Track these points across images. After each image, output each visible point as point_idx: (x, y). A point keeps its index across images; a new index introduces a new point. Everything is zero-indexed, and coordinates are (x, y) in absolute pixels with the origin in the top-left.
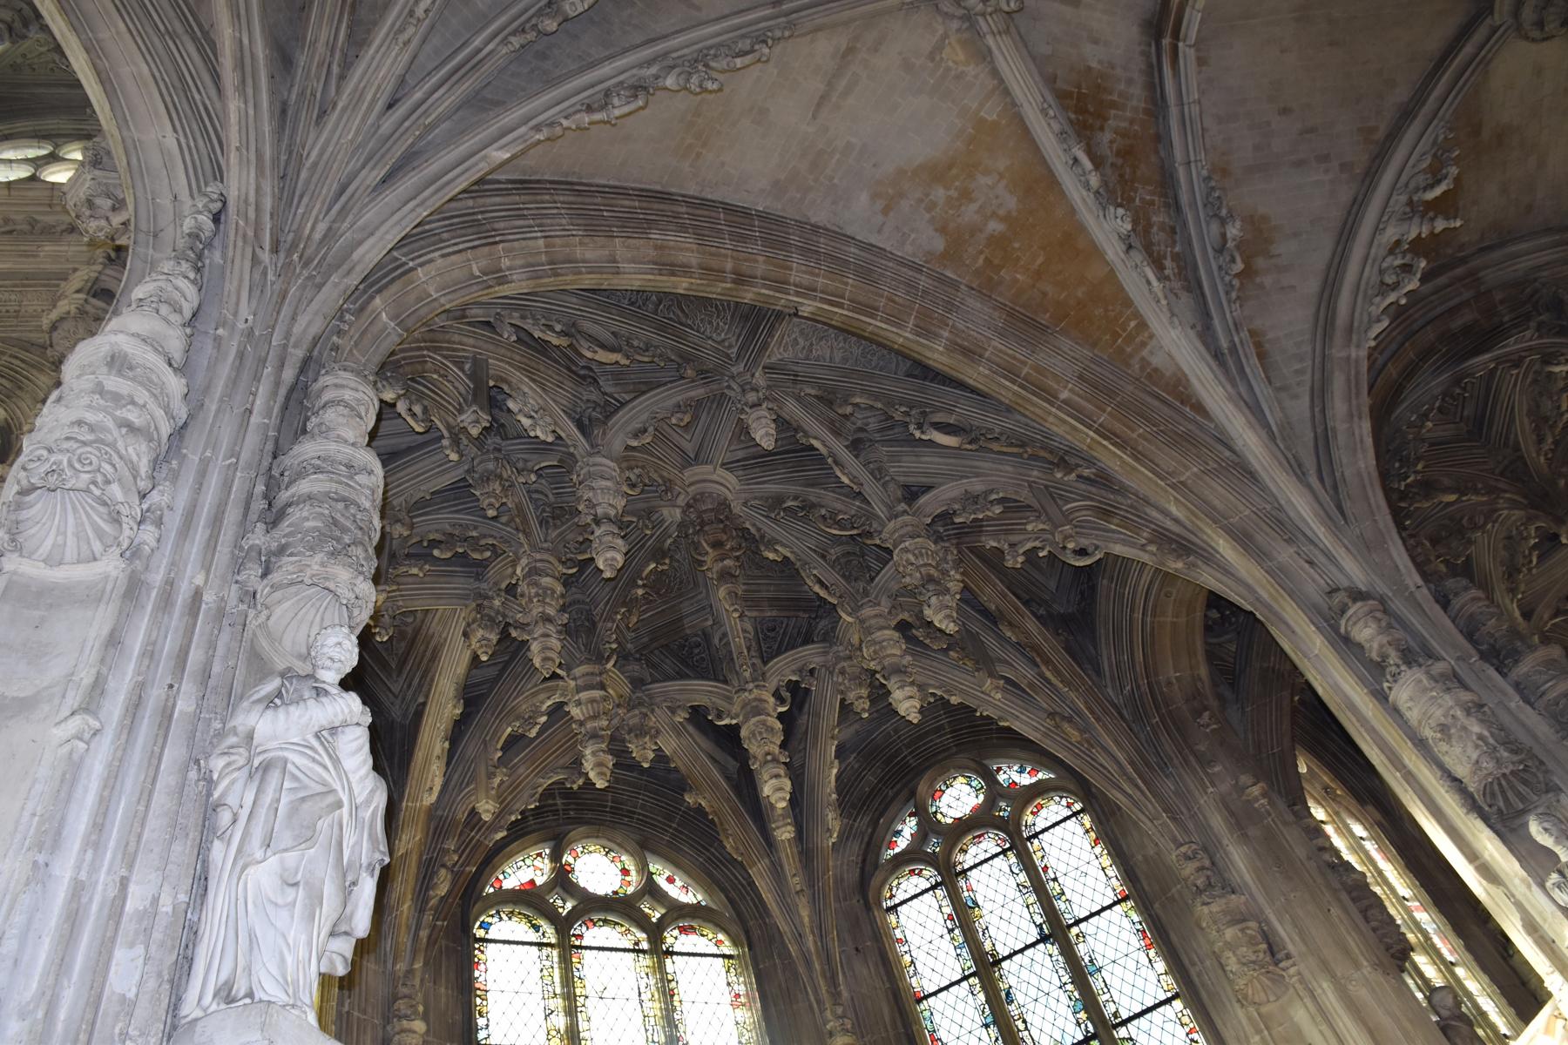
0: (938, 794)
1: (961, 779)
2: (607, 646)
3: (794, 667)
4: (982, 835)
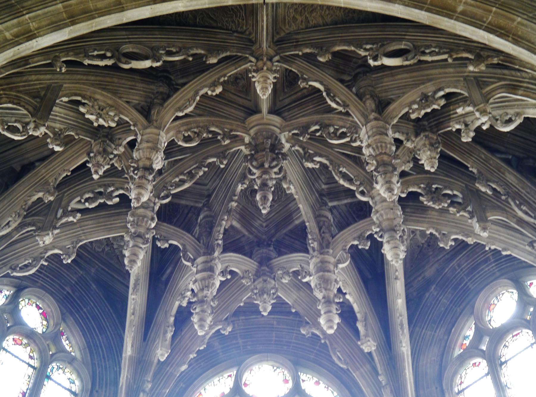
0: (492, 307)
1: (506, 294)
2: (216, 242)
3: (355, 235)
4: (519, 334)
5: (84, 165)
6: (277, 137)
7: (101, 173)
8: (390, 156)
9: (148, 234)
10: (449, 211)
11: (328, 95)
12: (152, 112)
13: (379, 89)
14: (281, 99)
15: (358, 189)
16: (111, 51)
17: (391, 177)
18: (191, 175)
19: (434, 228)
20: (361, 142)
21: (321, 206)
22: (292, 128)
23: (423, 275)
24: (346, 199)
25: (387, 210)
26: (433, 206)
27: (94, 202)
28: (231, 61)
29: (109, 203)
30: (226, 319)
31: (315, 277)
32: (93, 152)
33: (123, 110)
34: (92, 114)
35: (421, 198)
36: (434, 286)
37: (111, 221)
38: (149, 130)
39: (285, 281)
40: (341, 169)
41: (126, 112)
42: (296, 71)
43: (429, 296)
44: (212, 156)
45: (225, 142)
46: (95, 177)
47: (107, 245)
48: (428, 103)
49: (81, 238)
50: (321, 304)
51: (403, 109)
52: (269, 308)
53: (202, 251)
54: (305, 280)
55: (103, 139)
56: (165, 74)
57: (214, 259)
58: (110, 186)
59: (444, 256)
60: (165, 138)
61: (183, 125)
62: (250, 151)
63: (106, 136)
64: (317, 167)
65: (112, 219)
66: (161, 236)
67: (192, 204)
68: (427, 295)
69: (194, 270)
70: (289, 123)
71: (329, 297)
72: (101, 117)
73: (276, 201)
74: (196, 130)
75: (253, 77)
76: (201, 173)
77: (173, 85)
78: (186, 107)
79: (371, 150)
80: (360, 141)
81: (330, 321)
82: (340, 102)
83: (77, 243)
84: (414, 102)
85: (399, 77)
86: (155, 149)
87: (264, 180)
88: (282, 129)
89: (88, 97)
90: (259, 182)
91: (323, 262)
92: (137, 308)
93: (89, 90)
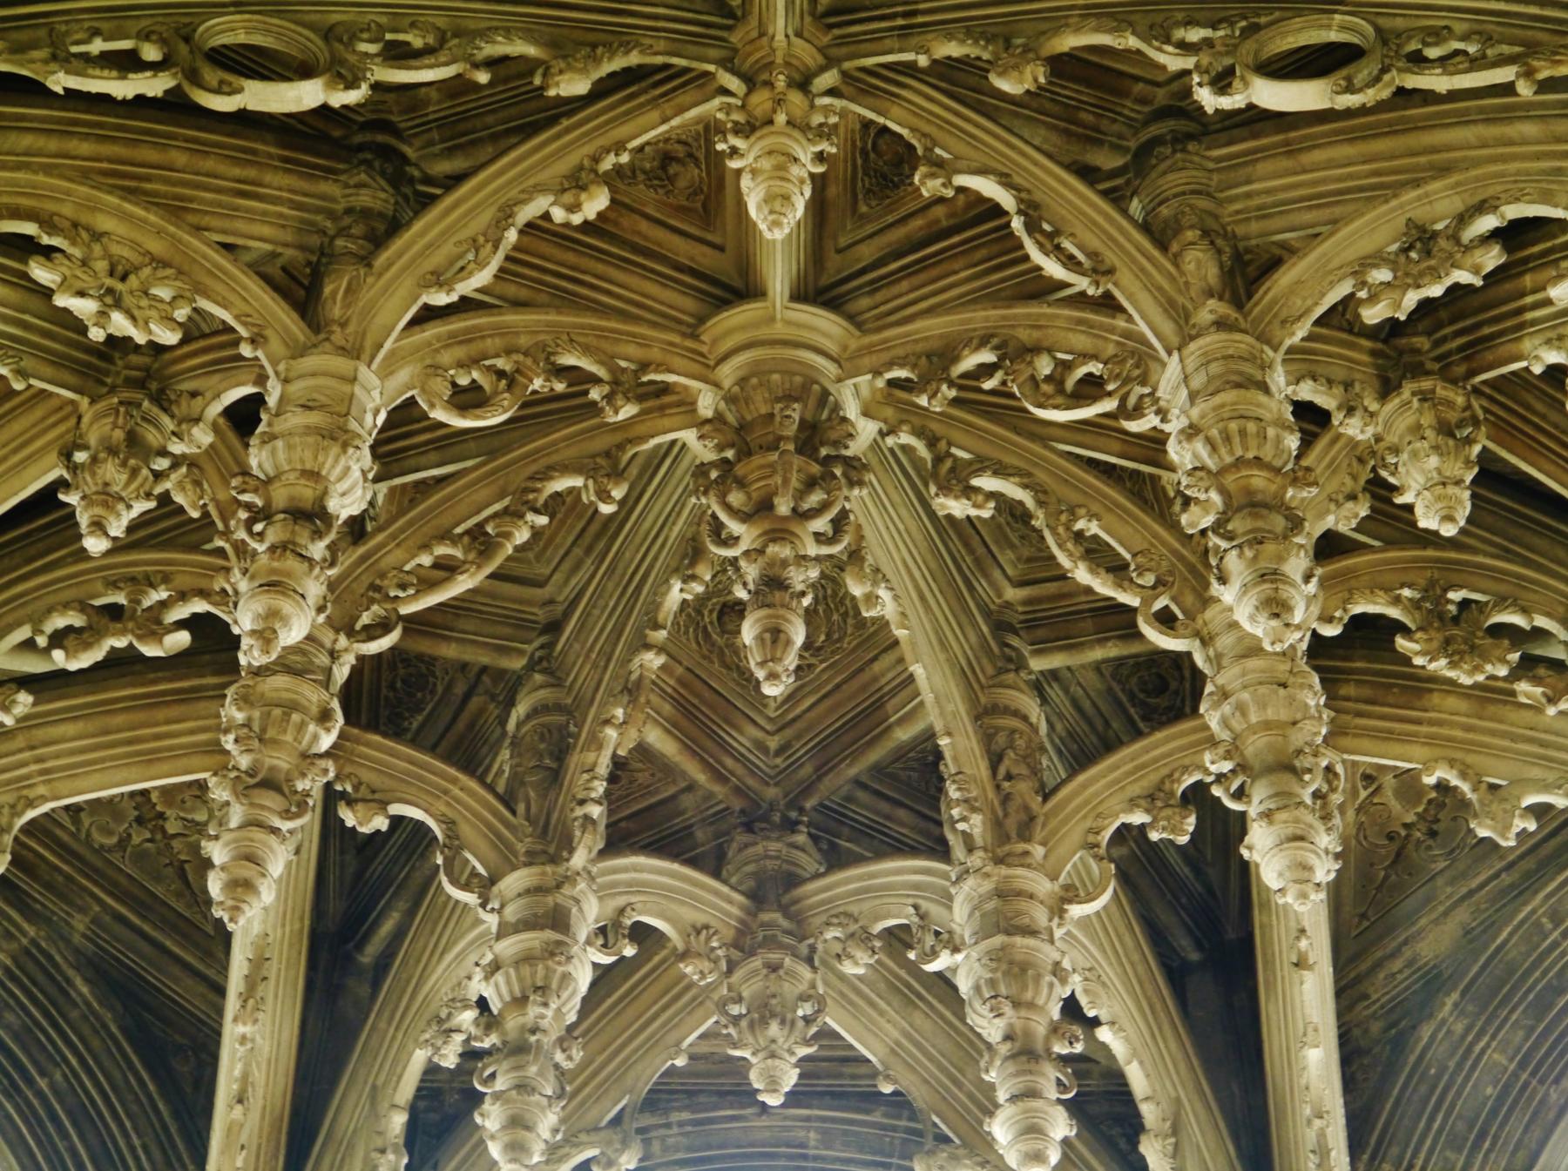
2: (579, 812)
3: (1136, 790)
5: (46, 499)
6: (825, 394)
7: (117, 528)
8: (1278, 471)
9: (304, 775)
10: (1513, 693)
11: (1032, 227)
12: (327, 290)
13: (1238, 206)
14: (843, 241)
15: (1147, 602)
16: (163, 41)
17: (1281, 559)
18: (483, 544)
19: (1452, 763)
20: (1163, 414)
21: (1001, 671)
22: (885, 357)
23: (1408, 953)
24: (1102, 642)
25: (1263, 690)
26: (1451, 674)
27: (87, 646)
28: (644, 91)
29: (150, 650)
30: (617, 1121)
31: (974, 955)
32: (85, 447)
33: (208, 281)
34: (81, 294)
35: (1401, 643)
36: (1455, 996)
37: (157, 724)
38: (312, 362)
39: (849, 968)
40: (1080, 525)
41: (220, 288)
42: (904, 132)
43: (1433, 1037)
44: (566, 469)
45: (616, 412)
46: (95, 545)
47: (140, 821)
48: (1433, 262)
49: (32, 794)
50: (998, 1063)
51: (1332, 284)
52: (790, 1078)
53: (521, 848)
54: (932, 967)
55: (127, 395)
56: (381, 138)
57: (569, 879)
58: (153, 586)
59: (1497, 875)
60: (376, 394)
61: (454, 340)
62: (720, 448)
63: (140, 384)
64: (986, 514)
65: (161, 714)
66: (356, 788)
67: (485, 659)
68: (1426, 1032)
69: (492, 921)
70: (875, 338)
71: (1028, 1034)
72: (118, 305)
73: (819, 649)
74: (501, 363)
75: (734, 151)
76: (522, 536)
77: (411, 180)
78: (463, 272)
79: (1199, 446)
80: (1158, 412)
81: (1032, 1130)
82: (1081, 257)
83: (17, 814)
84: (1376, 259)
85: (1318, 156)
86: (338, 435)
87: (771, 564)
88: (848, 364)
89: (67, 224)
90: (751, 571)
91: (1004, 893)
92: (259, 1076)
93: (70, 197)
